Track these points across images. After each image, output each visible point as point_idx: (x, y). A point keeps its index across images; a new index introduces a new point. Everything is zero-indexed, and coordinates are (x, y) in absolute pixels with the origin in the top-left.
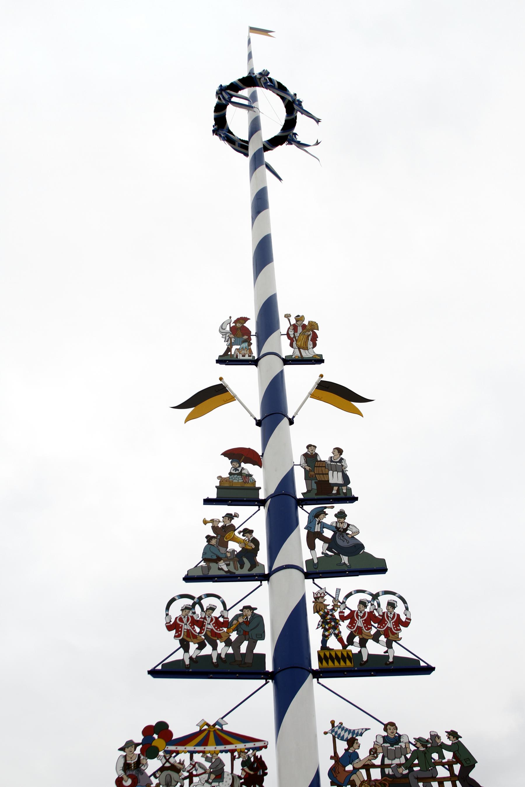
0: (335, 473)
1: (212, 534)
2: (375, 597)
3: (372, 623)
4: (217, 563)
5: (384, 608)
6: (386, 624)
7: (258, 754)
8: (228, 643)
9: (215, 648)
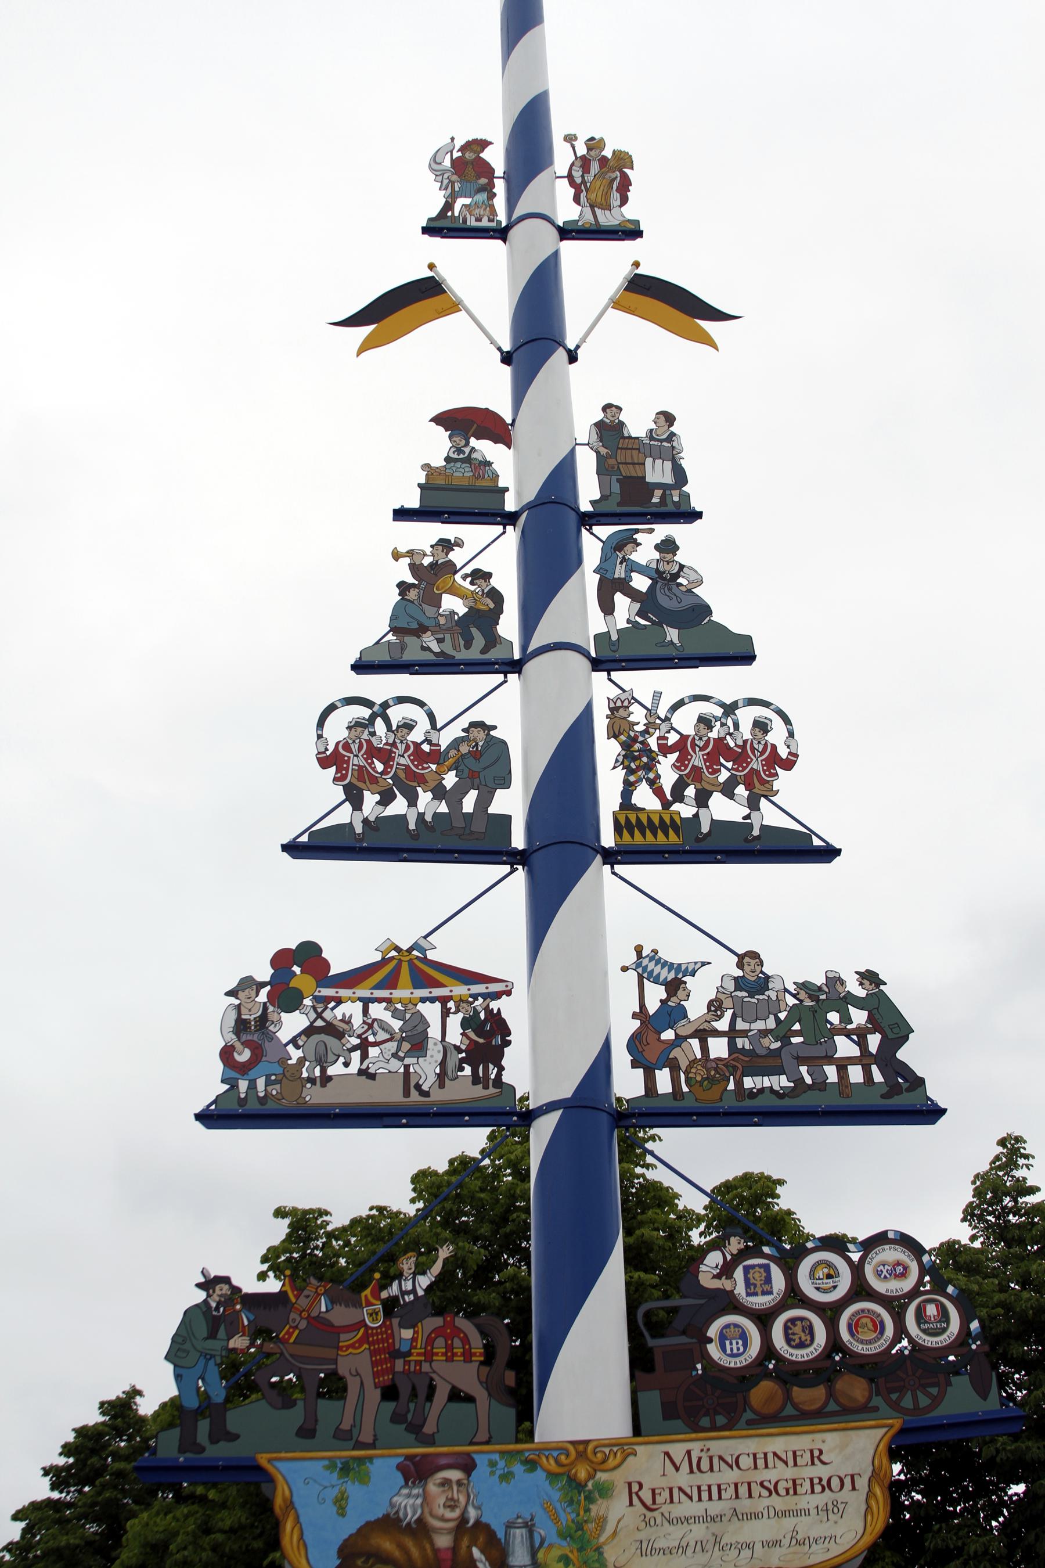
0: (659, 462)
1: (410, 580)
2: (730, 709)
3: (722, 760)
4: (419, 637)
5: (746, 731)
6: (748, 764)
7: (494, 1005)
8: (439, 793)
9: (412, 802)
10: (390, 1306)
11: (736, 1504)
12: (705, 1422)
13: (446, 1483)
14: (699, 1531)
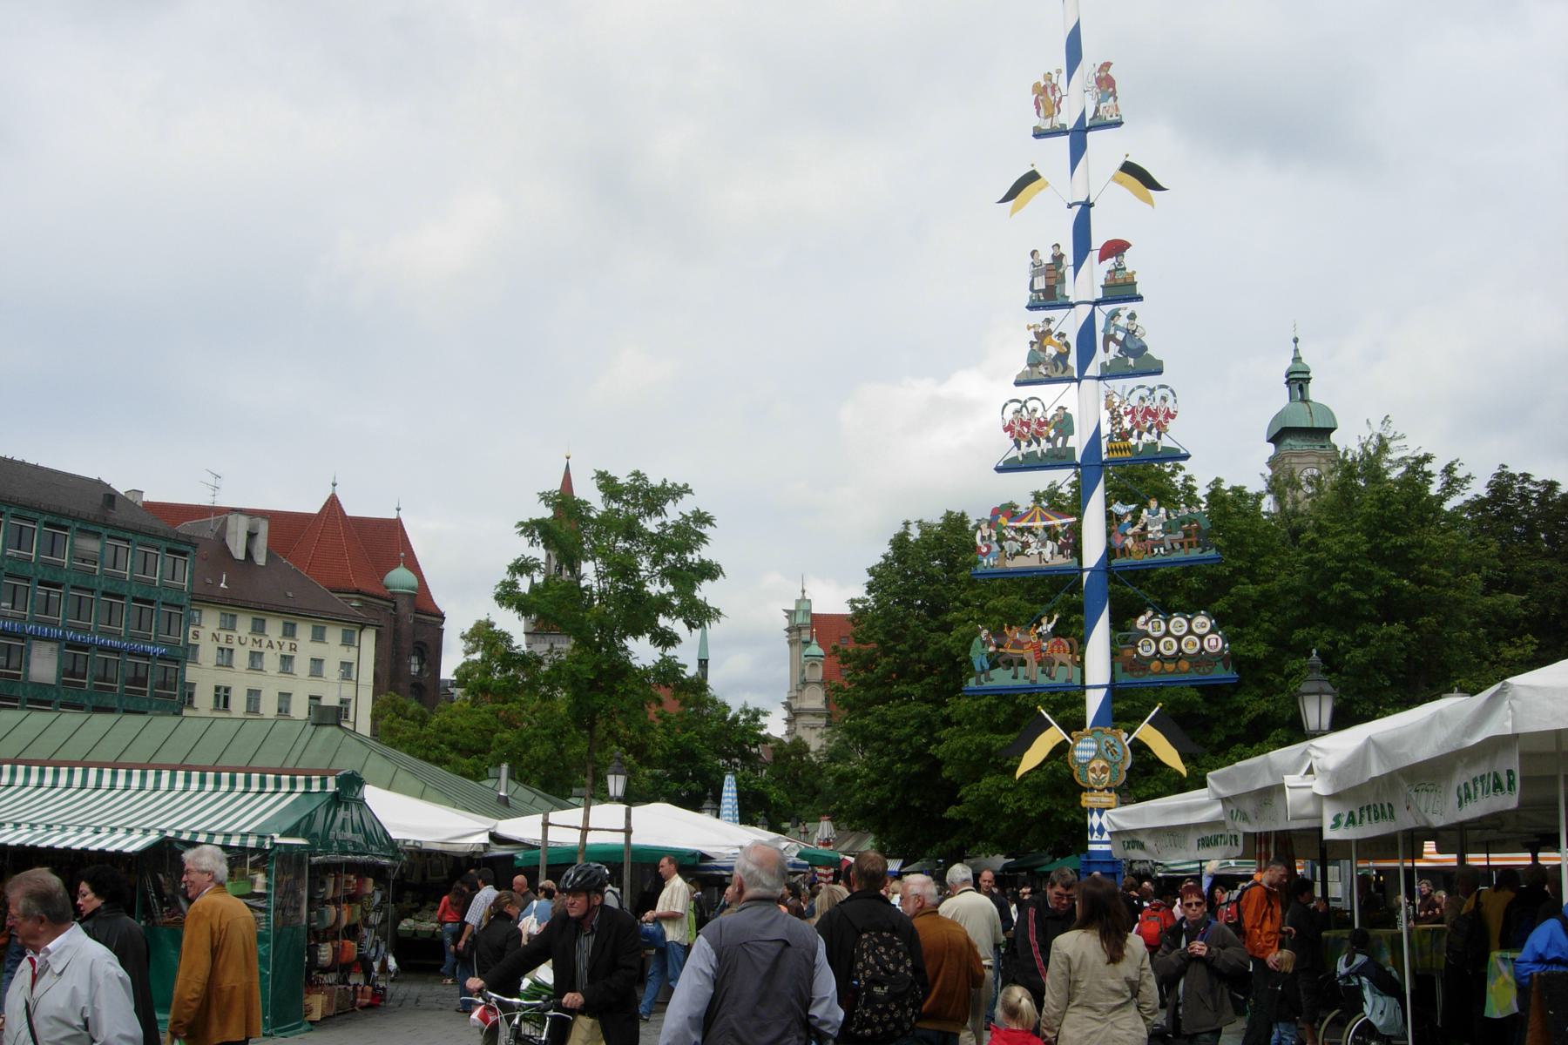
10: (1040, 635)
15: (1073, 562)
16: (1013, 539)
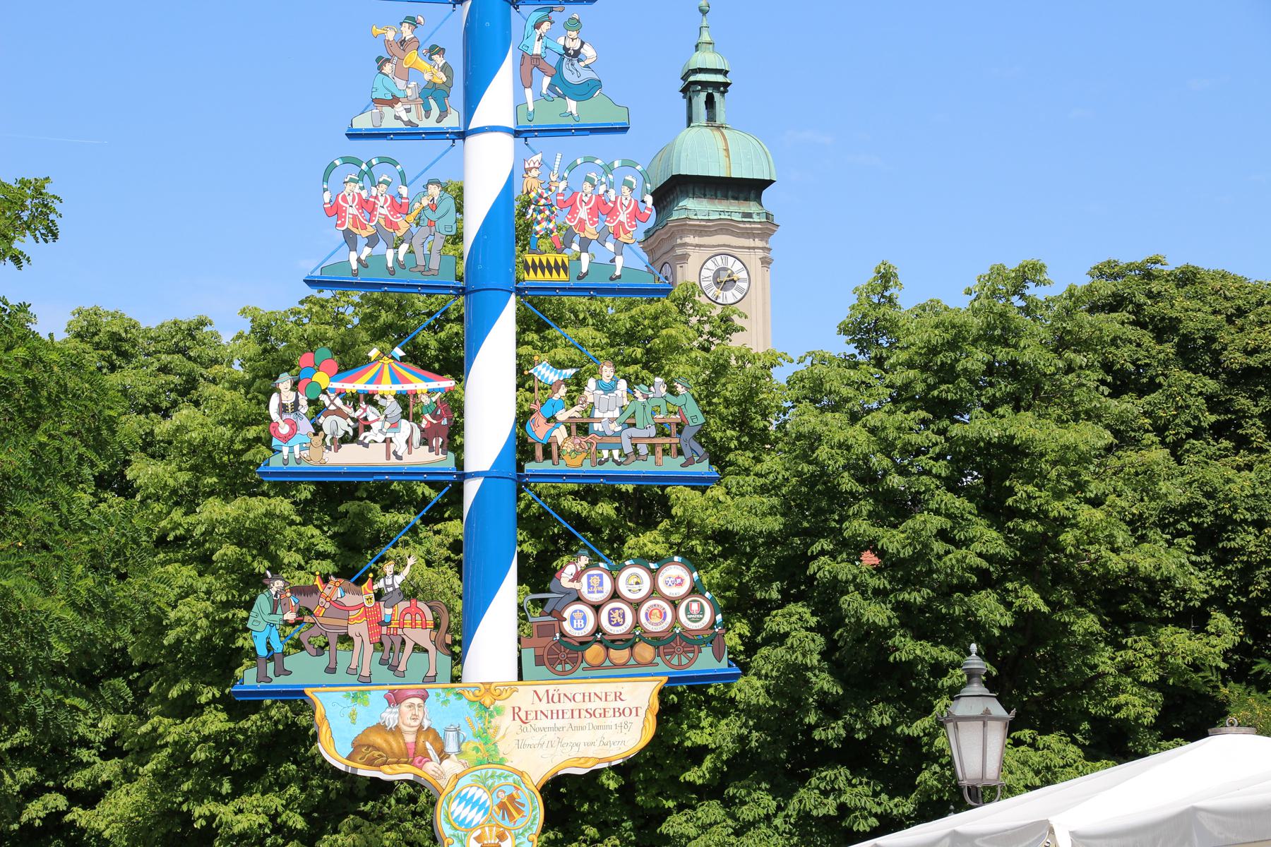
11: (571, 721)
12: (559, 668)
13: (412, 705)
14: (550, 736)
15: (446, 462)
16: (338, 412)
